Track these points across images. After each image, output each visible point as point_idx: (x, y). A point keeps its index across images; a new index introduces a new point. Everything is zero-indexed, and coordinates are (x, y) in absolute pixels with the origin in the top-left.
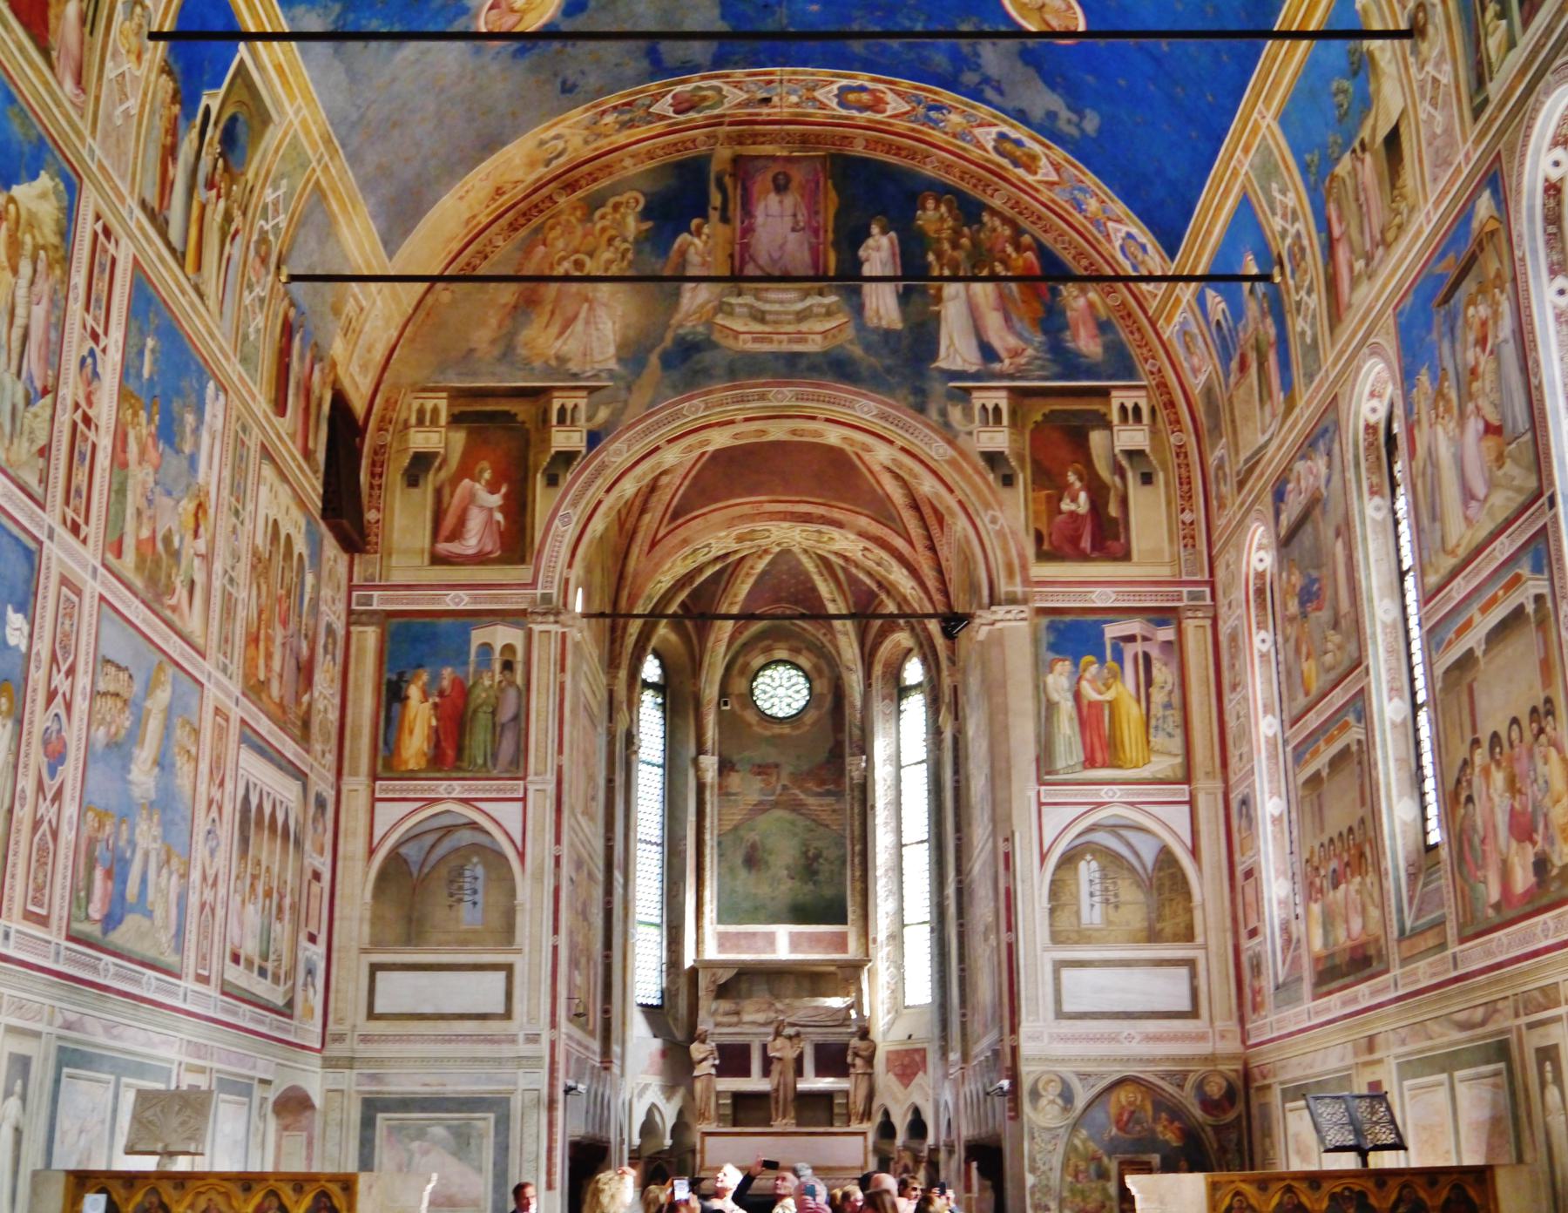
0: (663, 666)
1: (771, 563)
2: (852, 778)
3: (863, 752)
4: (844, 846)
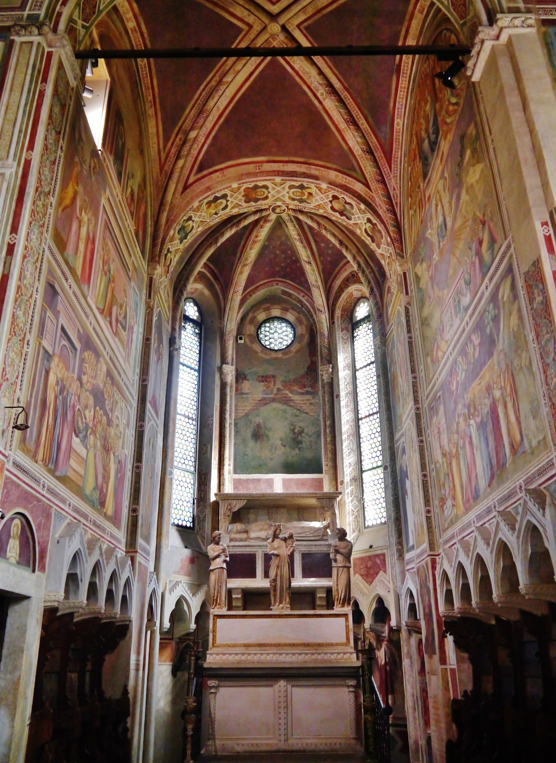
0: (200, 311)
1: (269, 238)
2: (323, 380)
3: (330, 362)
4: (319, 425)
